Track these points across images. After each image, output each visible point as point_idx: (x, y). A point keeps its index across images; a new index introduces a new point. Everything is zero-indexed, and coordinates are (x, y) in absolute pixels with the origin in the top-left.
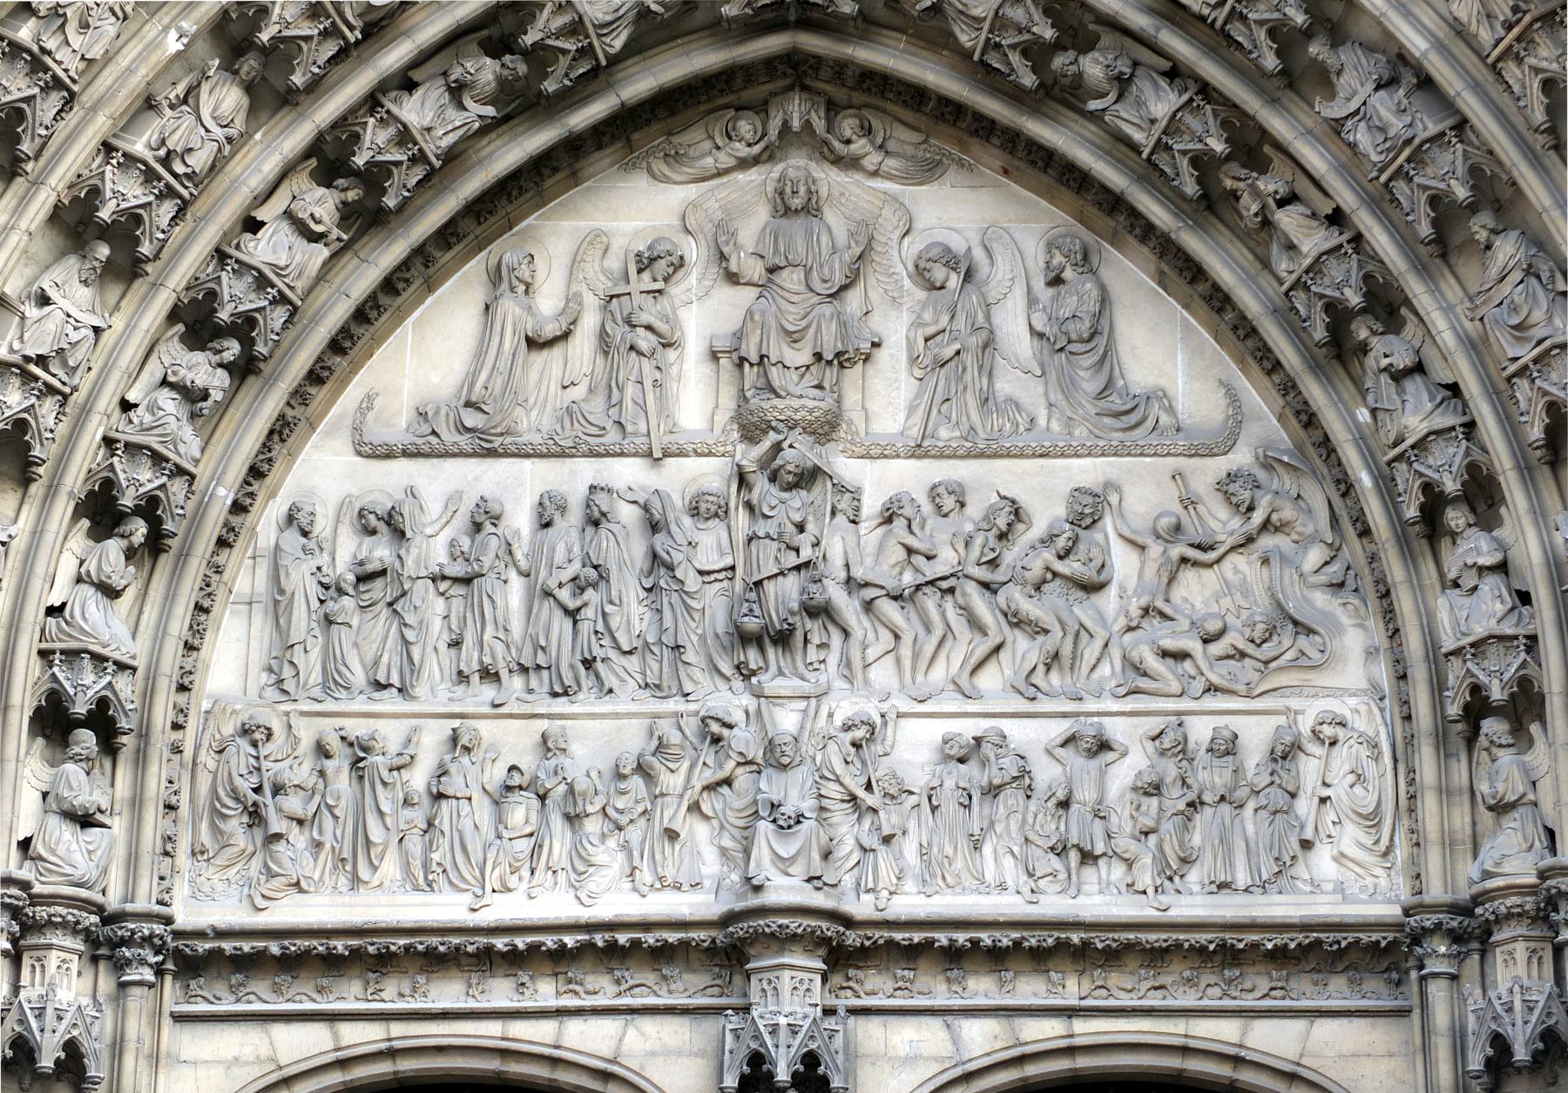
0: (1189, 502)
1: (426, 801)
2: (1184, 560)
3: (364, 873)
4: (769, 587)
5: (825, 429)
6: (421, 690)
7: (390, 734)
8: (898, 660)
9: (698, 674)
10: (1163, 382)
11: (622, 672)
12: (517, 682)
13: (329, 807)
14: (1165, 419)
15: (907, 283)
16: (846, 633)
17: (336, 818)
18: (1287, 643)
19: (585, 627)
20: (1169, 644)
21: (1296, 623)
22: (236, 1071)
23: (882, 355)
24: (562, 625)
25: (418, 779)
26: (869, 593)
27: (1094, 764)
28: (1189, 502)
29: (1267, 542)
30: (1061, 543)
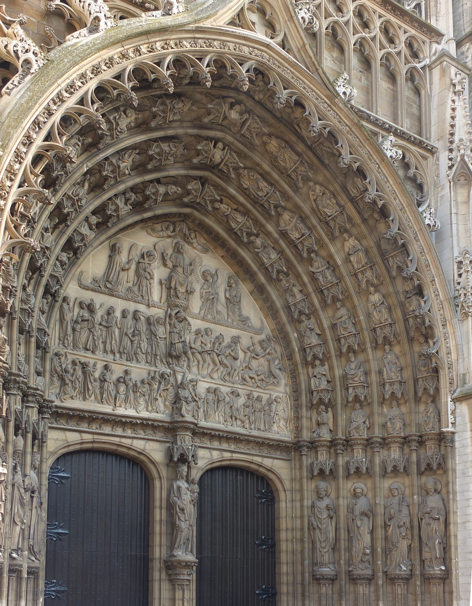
0: (253, 344)
1: (98, 381)
2: (253, 357)
3: (87, 397)
4: (176, 345)
5: (186, 309)
6: (97, 353)
7: (92, 362)
8: (198, 368)
9: (159, 362)
10: (249, 316)
11: (142, 357)
12: (118, 355)
13: (77, 379)
14: (250, 324)
15: (200, 277)
16: (189, 359)
17: (79, 382)
18: (271, 379)
19: (135, 345)
20: (251, 375)
21: (273, 375)
22: (57, 442)
23: (195, 293)
24: (129, 343)
25: (97, 375)
26: (194, 351)
27: (236, 399)
28: (253, 344)
29: (268, 357)
30: (233, 348)
